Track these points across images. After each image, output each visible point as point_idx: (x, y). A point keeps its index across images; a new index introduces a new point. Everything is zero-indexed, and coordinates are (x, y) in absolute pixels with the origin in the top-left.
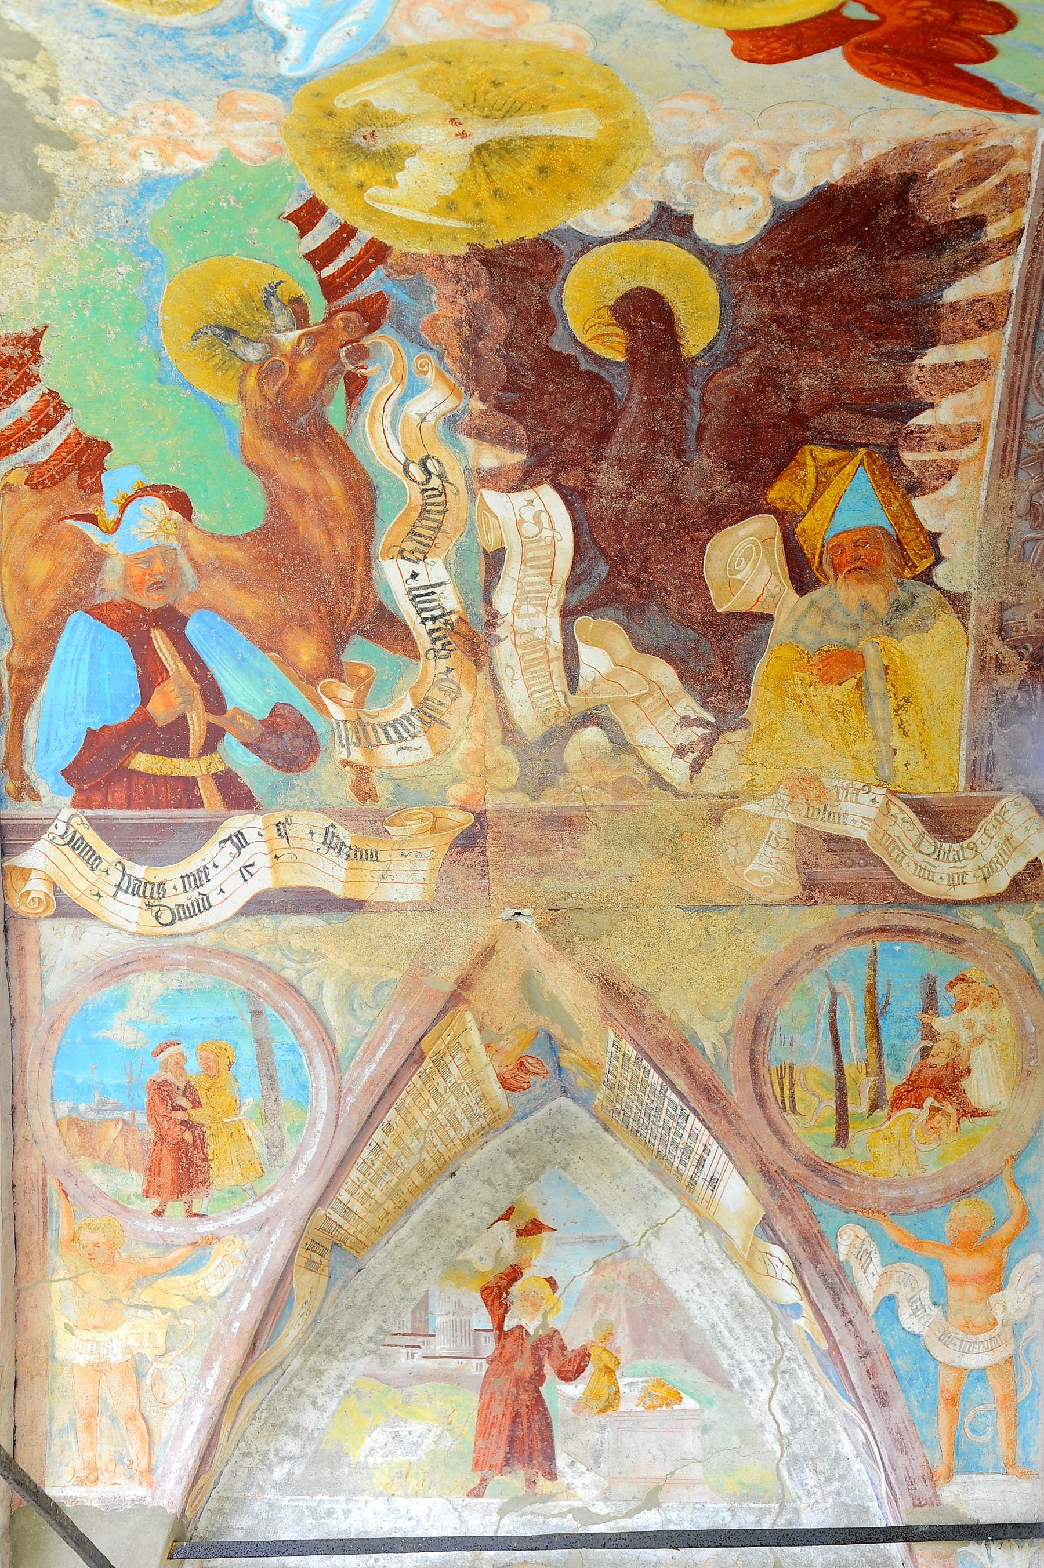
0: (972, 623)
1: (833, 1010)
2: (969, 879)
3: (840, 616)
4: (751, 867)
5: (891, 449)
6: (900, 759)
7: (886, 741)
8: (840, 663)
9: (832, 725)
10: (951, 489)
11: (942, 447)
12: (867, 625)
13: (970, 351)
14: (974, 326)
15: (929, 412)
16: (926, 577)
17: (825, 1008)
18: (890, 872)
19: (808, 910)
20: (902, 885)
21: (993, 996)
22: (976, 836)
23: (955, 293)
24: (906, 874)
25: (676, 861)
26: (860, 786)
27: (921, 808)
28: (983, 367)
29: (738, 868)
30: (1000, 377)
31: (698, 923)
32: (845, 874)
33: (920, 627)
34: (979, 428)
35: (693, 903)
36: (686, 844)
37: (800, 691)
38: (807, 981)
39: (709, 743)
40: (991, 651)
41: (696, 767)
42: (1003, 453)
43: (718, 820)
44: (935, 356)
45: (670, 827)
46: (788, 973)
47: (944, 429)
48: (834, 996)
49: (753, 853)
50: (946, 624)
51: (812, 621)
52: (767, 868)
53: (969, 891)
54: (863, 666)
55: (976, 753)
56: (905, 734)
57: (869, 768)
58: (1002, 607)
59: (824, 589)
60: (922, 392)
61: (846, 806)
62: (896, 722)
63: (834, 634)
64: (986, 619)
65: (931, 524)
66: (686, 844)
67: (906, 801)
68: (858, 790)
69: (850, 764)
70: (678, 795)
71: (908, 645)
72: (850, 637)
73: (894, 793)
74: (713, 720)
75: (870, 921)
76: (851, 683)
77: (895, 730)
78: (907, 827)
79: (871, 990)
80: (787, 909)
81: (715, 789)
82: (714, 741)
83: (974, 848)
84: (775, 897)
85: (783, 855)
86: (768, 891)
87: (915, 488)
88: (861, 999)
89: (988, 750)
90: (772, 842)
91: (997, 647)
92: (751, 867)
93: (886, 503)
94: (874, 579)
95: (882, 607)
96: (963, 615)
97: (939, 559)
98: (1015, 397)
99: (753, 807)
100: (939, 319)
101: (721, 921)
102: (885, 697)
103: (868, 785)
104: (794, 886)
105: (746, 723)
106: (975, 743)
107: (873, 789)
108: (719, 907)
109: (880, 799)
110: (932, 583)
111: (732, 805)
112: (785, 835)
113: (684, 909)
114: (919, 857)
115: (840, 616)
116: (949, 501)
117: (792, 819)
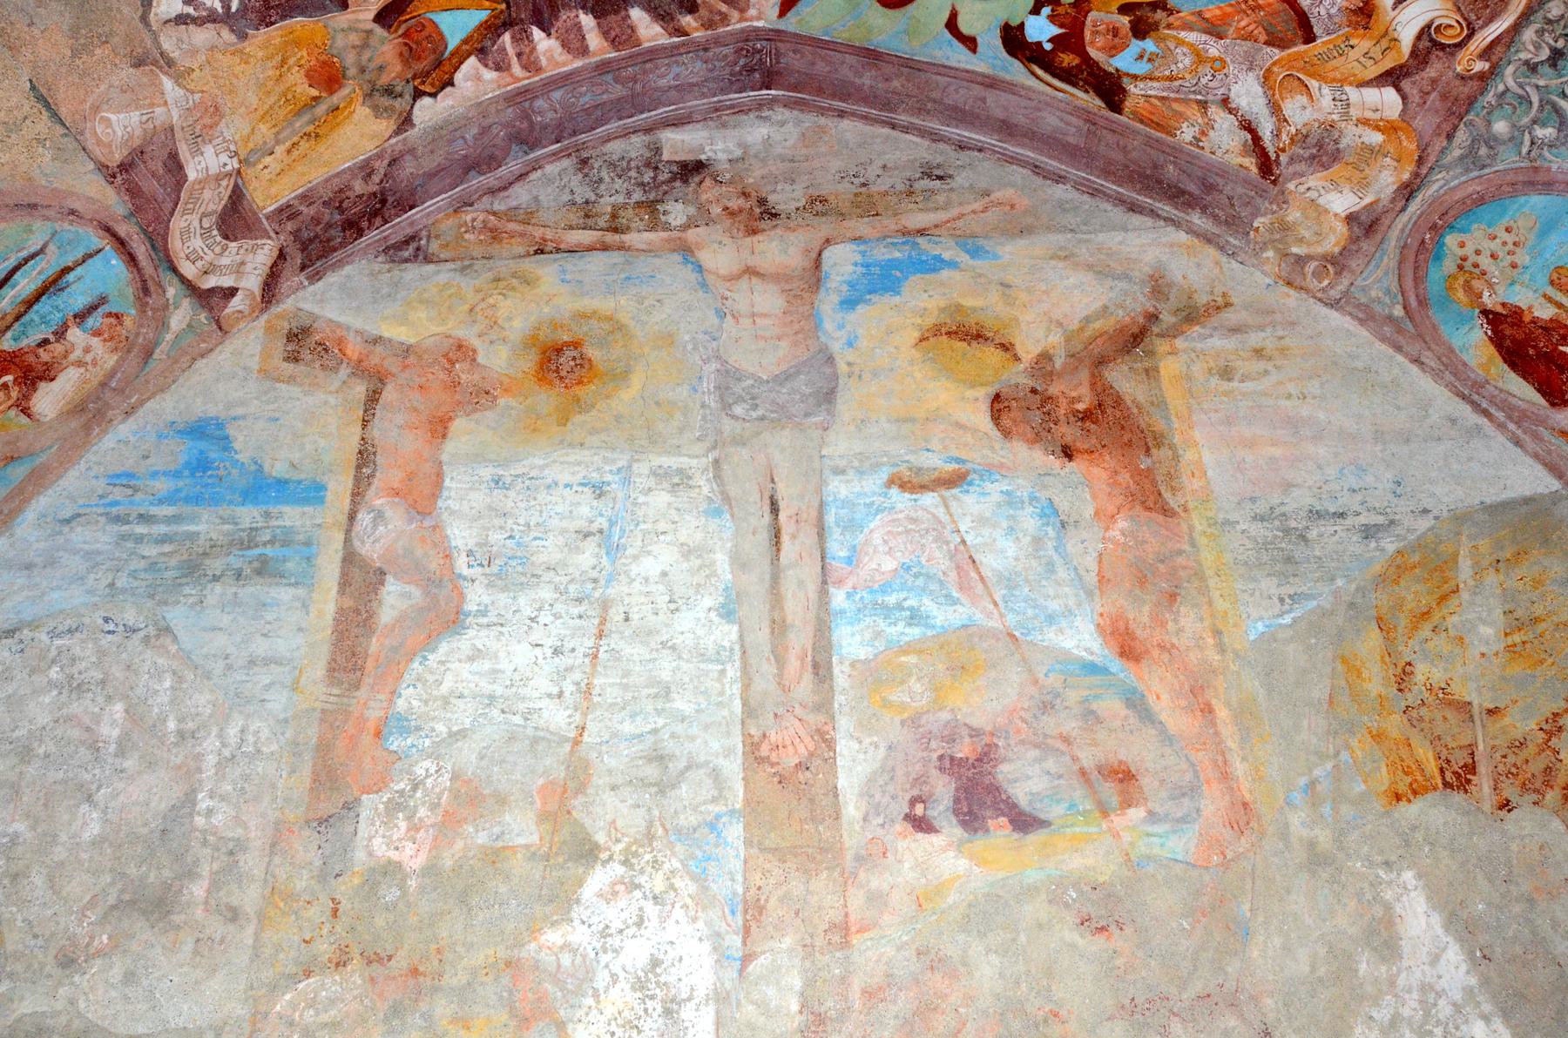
0: (393, 141)
1: (26, 261)
2: (199, 264)
3: (365, 58)
4: (113, 117)
5: (508, 24)
6: (268, 160)
7: (278, 142)
8: (328, 77)
9: (272, 100)
10: (489, 75)
11: (519, 55)
12: (367, 77)
13: (594, 40)
14: (613, 34)
15: (543, 35)
16: (418, 94)
17: (24, 254)
18: (172, 214)
19: (104, 183)
20: (168, 227)
21: (122, 345)
22: (234, 244)
23: (637, 14)
24: (178, 223)
25: (76, 54)
26: (232, 148)
27: (237, 196)
28: (584, 51)
29: (105, 107)
30: (578, 63)
31: (26, 108)
32: (149, 185)
33: (378, 111)
34: (539, 70)
35: (44, 91)
36: (98, 51)
37: (291, 61)
38: (37, 225)
39: (212, 18)
40: (377, 164)
41: (181, 20)
42: (524, 93)
43: (139, 63)
44: (587, 21)
45: (107, 29)
46: (33, 206)
47: (533, 49)
48: (41, 251)
49: (126, 108)
50: (385, 126)
51: (354, 38)
52: (119, 127)
53: (188, 270)
54: (331, 92)
55: (296, 202)
56: (289, 152)
57: (251, 145)
58: (411, 151)
59: (385, 34)
60: (559, 24)
61: (209, 151)
62: (295, 139)
63: (350, 59)
64: (400, 147)
65: (459, 77)
66: (98, 51)
67: (236, 185)
68: (228, 149)
69: (247, 130)
70: (144, 18)
71: (362, 112)
72: (352, 72)
73: (239, 172)
74: (234, 9)
75: (122, 230)
76: (314, 92)
77: (288, 144)
78: (214, 200)
79: (66, 270)
80: (92, 166)
81: (167, 44)
82: (214, 21)
83: (225, 249)
84: (98, 152)
85: (138, 132)
86: (99, 142)
87: (482, 52)
88: (51, 272)
89: (302, 208)
90: (145, 118)
91: (381, 166)
92: (113, 117)
93: (465, 41)
94: (406, 63)
95: (384, 80)
96: (399, 131)
97: (434, 95)
98: (565, 79)
99: (167, 83)
100: (616, 12)
101: (43, 124)
102: (312, 122)
103: (236, 153)
104: (118, 157)
105: (243, 37)
106: (304, 197)
107: (235, 160)
108: (56, 116)
109: (229, 168)
110: (415, 100)
111: (161, 68)
112: (158, 123)
113: (33, 88)
114: (196, 224)
115: (367, 55)
116: (479, 78)
117: (175, 118)
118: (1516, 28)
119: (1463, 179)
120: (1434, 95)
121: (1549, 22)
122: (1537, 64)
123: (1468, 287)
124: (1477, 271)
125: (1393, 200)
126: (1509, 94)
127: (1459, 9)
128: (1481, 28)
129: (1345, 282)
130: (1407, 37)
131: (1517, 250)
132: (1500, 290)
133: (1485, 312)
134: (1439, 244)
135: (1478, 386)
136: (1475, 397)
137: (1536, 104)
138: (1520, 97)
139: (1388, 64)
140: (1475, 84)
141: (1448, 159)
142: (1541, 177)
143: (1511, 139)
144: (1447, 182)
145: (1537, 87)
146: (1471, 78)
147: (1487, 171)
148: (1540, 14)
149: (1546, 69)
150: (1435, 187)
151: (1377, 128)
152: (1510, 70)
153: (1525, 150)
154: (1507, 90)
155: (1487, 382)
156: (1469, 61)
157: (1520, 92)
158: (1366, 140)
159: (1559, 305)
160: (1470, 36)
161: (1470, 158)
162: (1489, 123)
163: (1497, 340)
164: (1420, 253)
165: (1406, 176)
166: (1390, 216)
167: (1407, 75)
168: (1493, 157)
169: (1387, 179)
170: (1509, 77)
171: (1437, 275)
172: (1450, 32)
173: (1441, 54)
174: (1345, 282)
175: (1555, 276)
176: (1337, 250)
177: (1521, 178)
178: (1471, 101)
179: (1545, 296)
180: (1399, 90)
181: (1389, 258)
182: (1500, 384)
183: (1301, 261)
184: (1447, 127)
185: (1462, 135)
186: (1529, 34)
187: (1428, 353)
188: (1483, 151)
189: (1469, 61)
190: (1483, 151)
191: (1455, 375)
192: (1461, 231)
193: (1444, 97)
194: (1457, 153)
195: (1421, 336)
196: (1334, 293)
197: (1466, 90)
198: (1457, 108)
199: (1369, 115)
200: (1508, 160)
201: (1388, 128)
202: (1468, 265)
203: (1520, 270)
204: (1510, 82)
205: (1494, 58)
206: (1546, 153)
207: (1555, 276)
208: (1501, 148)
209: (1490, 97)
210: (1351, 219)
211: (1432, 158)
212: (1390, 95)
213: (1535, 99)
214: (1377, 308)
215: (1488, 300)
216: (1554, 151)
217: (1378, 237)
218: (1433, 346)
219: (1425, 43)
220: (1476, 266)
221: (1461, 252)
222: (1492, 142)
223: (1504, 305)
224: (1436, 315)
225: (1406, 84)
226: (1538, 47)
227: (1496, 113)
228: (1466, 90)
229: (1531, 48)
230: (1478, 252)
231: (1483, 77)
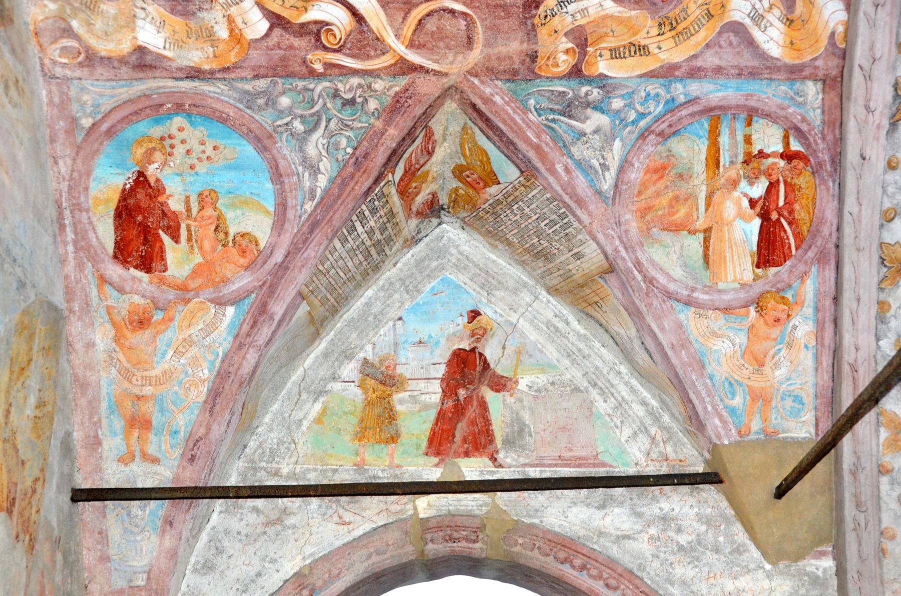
118: (355, 72)
119: (232, 102)
120: (282, 52)
121: (369, 87)
122: (339, 96)
123: (150, 153)
124: (169, 150)
125: (180, 69)
126: (310, 93)
127: (349, 35)
128: (345, 54)
129: (78, 73)
130: (314, 14)
131: (205, 162)
132: (167, 171)
133: (141, 174)
134: (170, 115)
135: (77, 207)
136: (67, 213)
137: (313, 111)
138: (313, 100)
139: (285, 13)
140: (304, 70)
141: (240, 85)
142: (267, 142)
143: (281, 112)
144: (222, 94)
145: (325, 104)
146: (307, 67)
147: (248, 111)
148: (371, 79)
149: (339, 102)
150: (212, 89)
151: (231, 31)
152: (327, 84)
153: (279, 123)
154: (313, 90)
155: (87, 211)
156: (317, 60)
157: (316, 98)
158: (217, 28)
159: (189, 209)
160: (335, 51)
161: (249, 99)
162: (284, 93)
163: (126, 195)
164: (154, 108)
165: (206, 67)
166: (165, 73)
167: (285, 29)
168: (260, 109)
169: (196, 56)
170: (321, 87)
171: (143, 127)
172: (331, 38)
173: (313, 41)
174: (78, 73)
175: (207, 193)
176: (103, 54)
177: (258, 133)
178: (292, 75)
179: (187, 197)
180: (271, 29)
181: (125, 92)
182: (94, 219)
183: (68, 32)
184: (262, 71)
185: (262, 84)
186: (355, 81)
187: (69, 162)
188: (261, 101)
189: (317, 60)
190: (261, 101)
191: (70, 188)
192: (192, 123)
193: (283, 59)
194: (248, 87)
195: (79, 149)
196: (59, 71)
197: (297, 68)
198: (280, 69)
199: (239, 21)
200: (266, 119)
201: (236, 36)
202: (167, 142)
203: (193, 172)
204: (319, 89)
205: (329, 71)
206: (285, 135)
207: (207, 193)
208: (270, 110)
209: (301, 84)
210: (141, 50)
211: (233, 75)
212: (264, 25)
213: (317, 108)
214: (75, 107)
215: (152, 171)
216: (290, 138)
217: (141, 75)
218: (79, 161)
219: (314, 28)
220: (172, 147)
221: (174, 131)
222: (271, 102)
223: (158, 180)
224: (109, 147)
225: (277, 32)
226: (350, 90)
227: (293, 94)
228: (297, 68)
229: (348, 87)
230: (183, 142)
231: (312, 73)
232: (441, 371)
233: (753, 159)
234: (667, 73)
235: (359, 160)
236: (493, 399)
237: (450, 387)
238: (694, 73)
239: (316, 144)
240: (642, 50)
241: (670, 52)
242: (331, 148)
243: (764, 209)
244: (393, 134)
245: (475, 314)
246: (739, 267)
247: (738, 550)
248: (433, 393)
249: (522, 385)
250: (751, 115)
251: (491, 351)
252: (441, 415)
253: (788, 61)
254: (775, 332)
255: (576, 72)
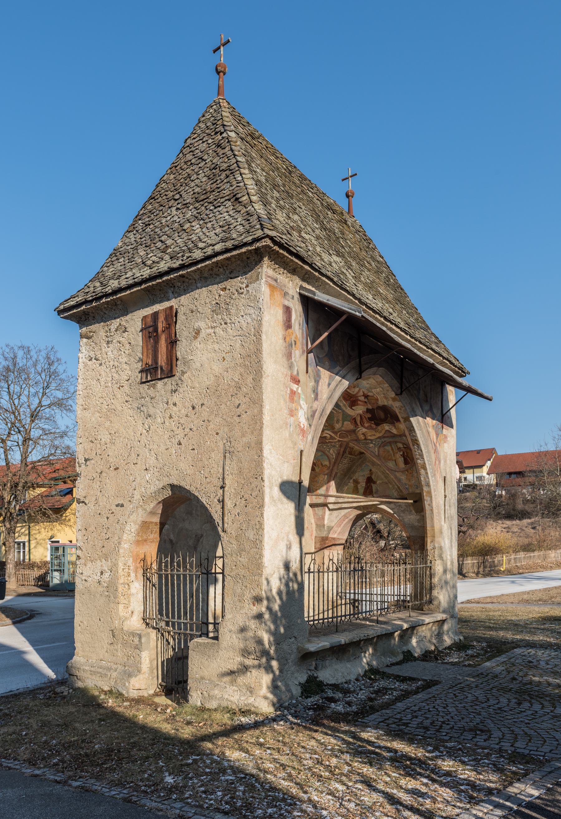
232: (365, 481)
233: (399, 449)
234: (379, 438)
235: (339, 453)
236: (373, 485)
237: (367, 483)
238: (384, 437)
239: (331, 451)
240: (375, 435)
241: (378, 435)
242: (334, 452)
243: (403, 456)
244: (342, 450)
245: (371, 470)
246: (402, 465)
247: (411, 511)
248: (364, 484)
249: (378, 483)
250: (396, 442)
251: (373, 477)
252: (365, 489)
253: (398, 434)
254: (411, 475)
255: (366, 439)
